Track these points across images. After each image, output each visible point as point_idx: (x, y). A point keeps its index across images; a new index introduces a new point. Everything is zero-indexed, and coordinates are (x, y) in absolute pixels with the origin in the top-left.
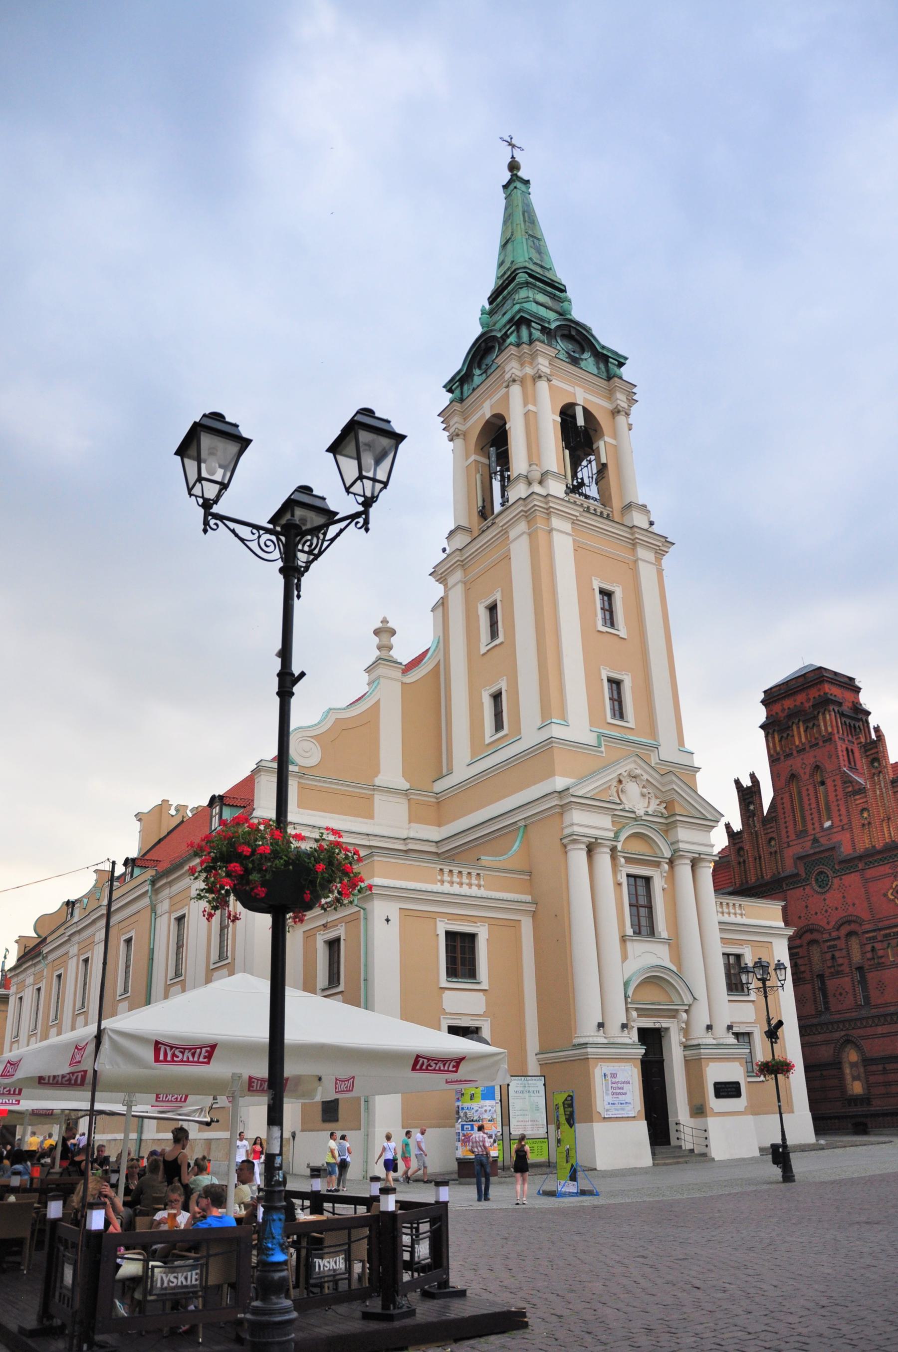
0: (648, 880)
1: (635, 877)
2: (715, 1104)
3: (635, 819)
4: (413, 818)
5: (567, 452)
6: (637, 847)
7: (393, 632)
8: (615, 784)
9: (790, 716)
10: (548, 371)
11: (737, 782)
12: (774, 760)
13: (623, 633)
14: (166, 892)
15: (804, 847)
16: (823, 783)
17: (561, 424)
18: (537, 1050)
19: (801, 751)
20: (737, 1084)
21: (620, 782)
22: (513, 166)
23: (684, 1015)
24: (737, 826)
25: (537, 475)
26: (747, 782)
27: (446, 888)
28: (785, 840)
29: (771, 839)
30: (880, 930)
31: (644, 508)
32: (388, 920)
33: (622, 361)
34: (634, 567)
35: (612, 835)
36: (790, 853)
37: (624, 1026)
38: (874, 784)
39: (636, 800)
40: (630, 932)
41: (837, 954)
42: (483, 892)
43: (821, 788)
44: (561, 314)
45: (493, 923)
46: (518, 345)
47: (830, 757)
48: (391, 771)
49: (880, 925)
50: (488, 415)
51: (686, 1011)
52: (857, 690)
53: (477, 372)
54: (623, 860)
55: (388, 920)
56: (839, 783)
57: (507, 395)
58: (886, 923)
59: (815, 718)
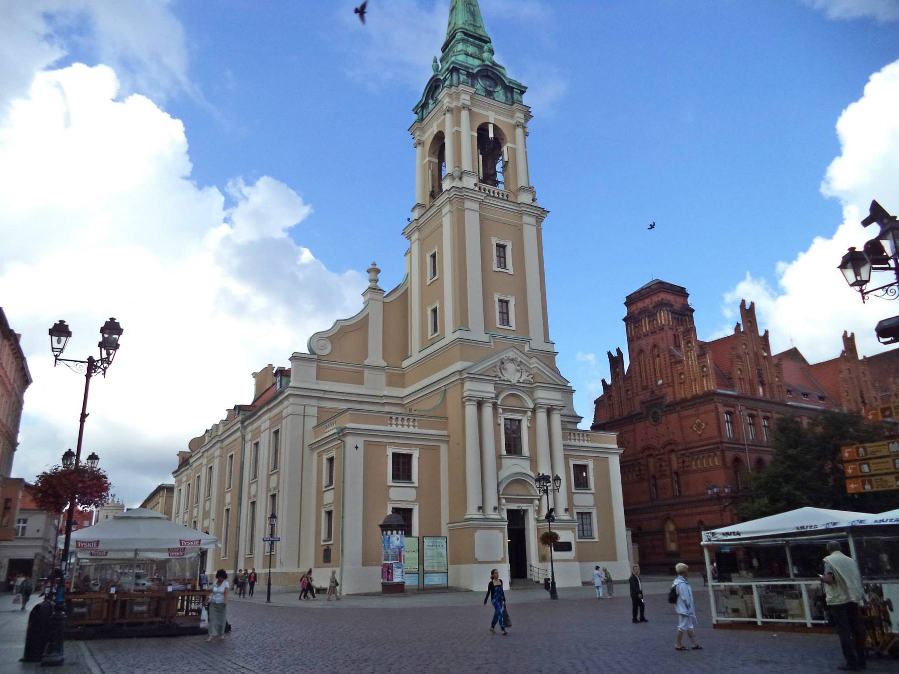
0: (520, 421)
1: (511, 420)
3: (511, 386)
4: (390, 384)
5: (481, 156)
6: (512, 402)
7: (378, 271)
8: (499, 364)
9: (640, 313)
10: (469, 103)
11: (609, 354)
12: (630, 341)
13: (511, 271)
14: (249, 429)
15: (644, 396)
16: (658, 356)
17: (478, 138)
18: (448, 521)
19: (646, 335)
20: (570, 543)
21: (503, 363)
23: (537, 502)
24: (609, 382)
25: (457, 174)
26: (615, 354)
27: (393, 428)
28: (635, 391)
29: (628, 391)
30: (687, 449)
31: (530, 189)
32: (356, 448)
34: (520, 229)
35: (494, 396)
36: (638, 400)
37: (495, 508)
38: (688, 358)
39: (512, 375)
40: (504, 452)
41: (663, 464)
42: (416, 430)
43: (658, 359)
44: (483, 61)
46: (451, 86)
47: (662, 339)
48: (375, 357)
49: (688, 446)
50: (435, 132)
51: (539, 500)
52: (687, 295)
53: (431, 102)
54: (501, 411)
55: (356, 448)
56: (667, 356)
57: (444, 121)
58: (691, 445)
59: (655, 314)
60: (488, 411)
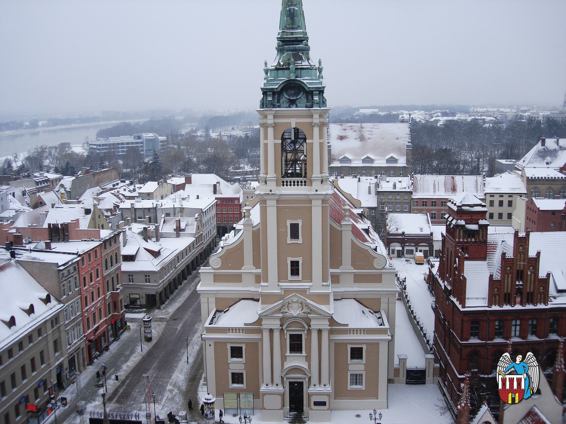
2: (313, 406)
33: (322, 89)
45: (247, 344)
60: (277, 335)
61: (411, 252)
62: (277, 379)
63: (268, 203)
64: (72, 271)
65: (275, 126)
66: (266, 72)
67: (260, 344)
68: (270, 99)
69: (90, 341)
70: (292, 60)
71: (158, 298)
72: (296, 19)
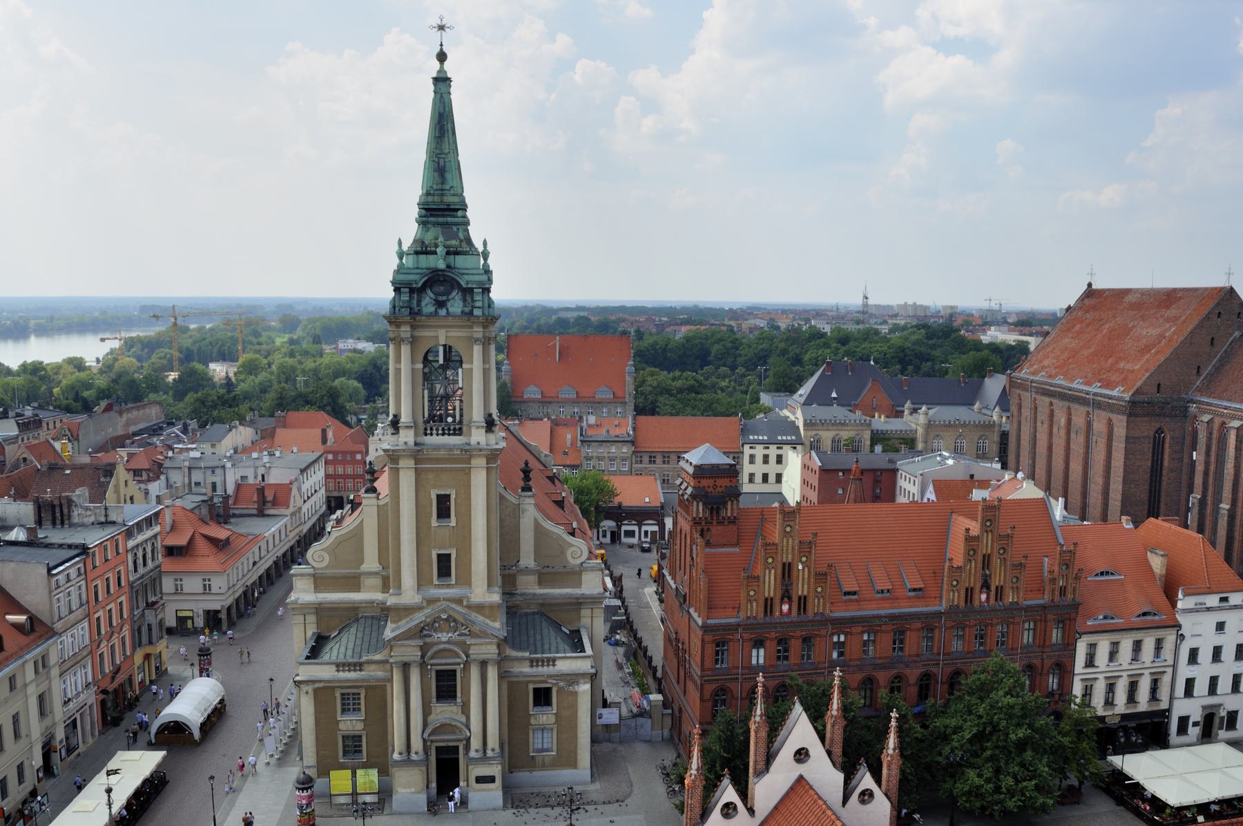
22: (442, 57)
34: (467, 472)
48: (371, 563)
61: (630, 534)
62: (417, 744)
63: (403, 463)
64: (73, 576)
65: (414, 341)
66: (401, 255)
67: (389, 685)
68: (405, 297)
69: (104, 692)
70: (441, 239)
71: (223, 616)
72: (448, 176)
